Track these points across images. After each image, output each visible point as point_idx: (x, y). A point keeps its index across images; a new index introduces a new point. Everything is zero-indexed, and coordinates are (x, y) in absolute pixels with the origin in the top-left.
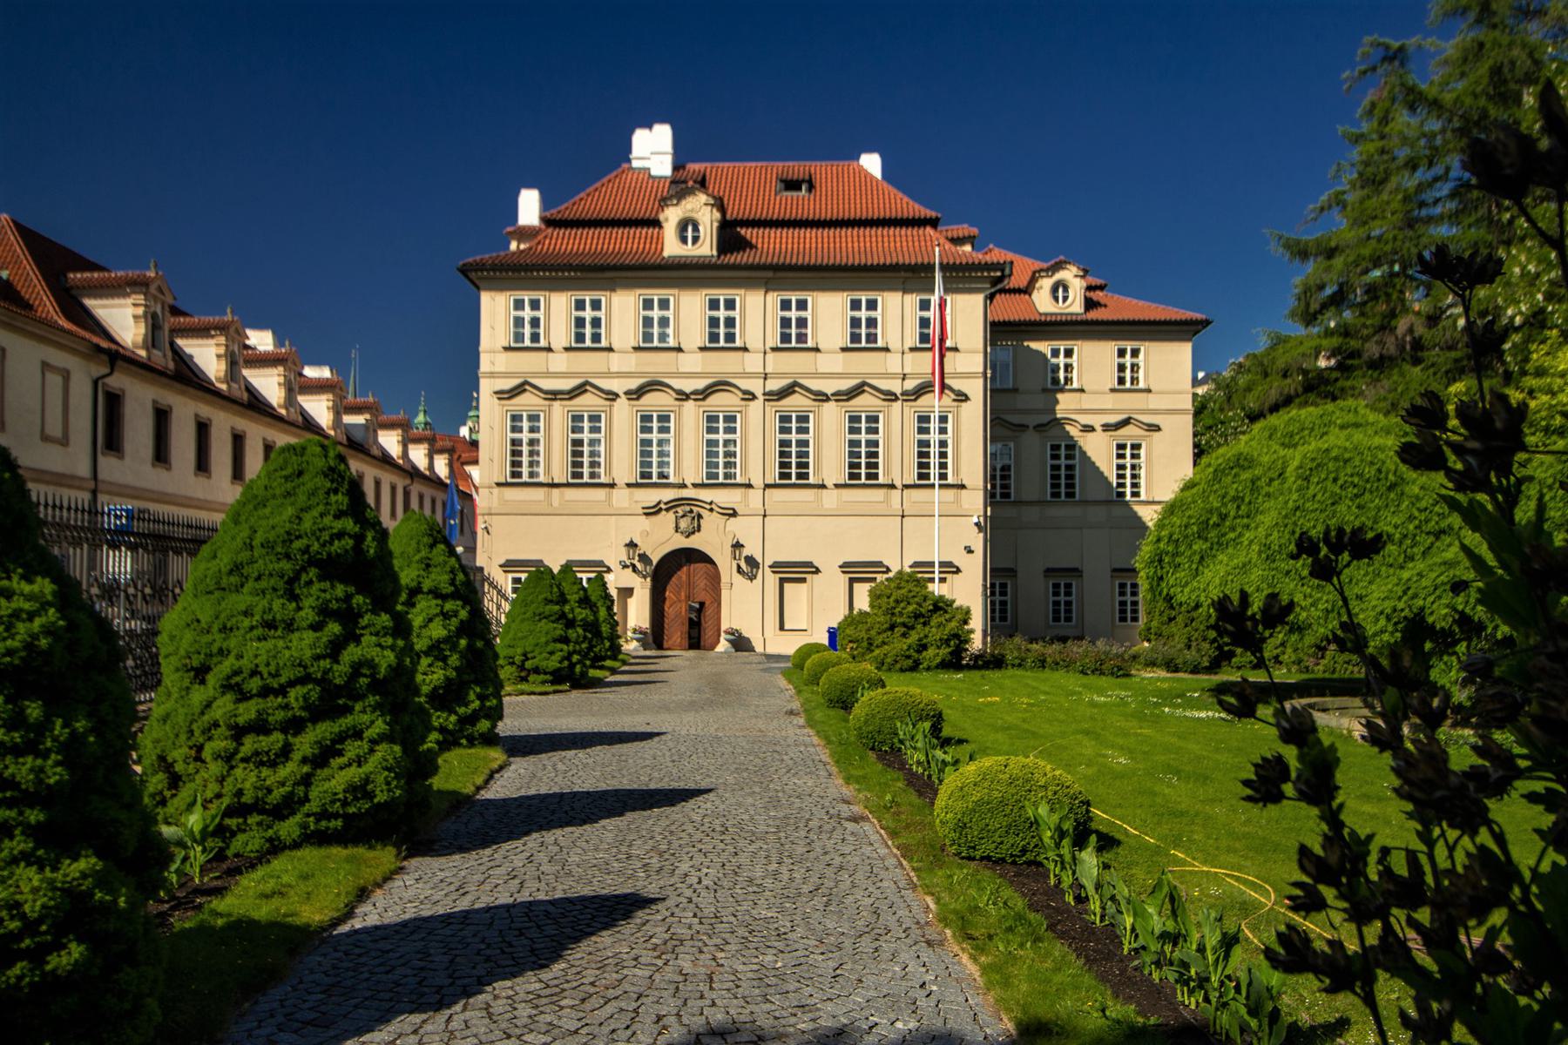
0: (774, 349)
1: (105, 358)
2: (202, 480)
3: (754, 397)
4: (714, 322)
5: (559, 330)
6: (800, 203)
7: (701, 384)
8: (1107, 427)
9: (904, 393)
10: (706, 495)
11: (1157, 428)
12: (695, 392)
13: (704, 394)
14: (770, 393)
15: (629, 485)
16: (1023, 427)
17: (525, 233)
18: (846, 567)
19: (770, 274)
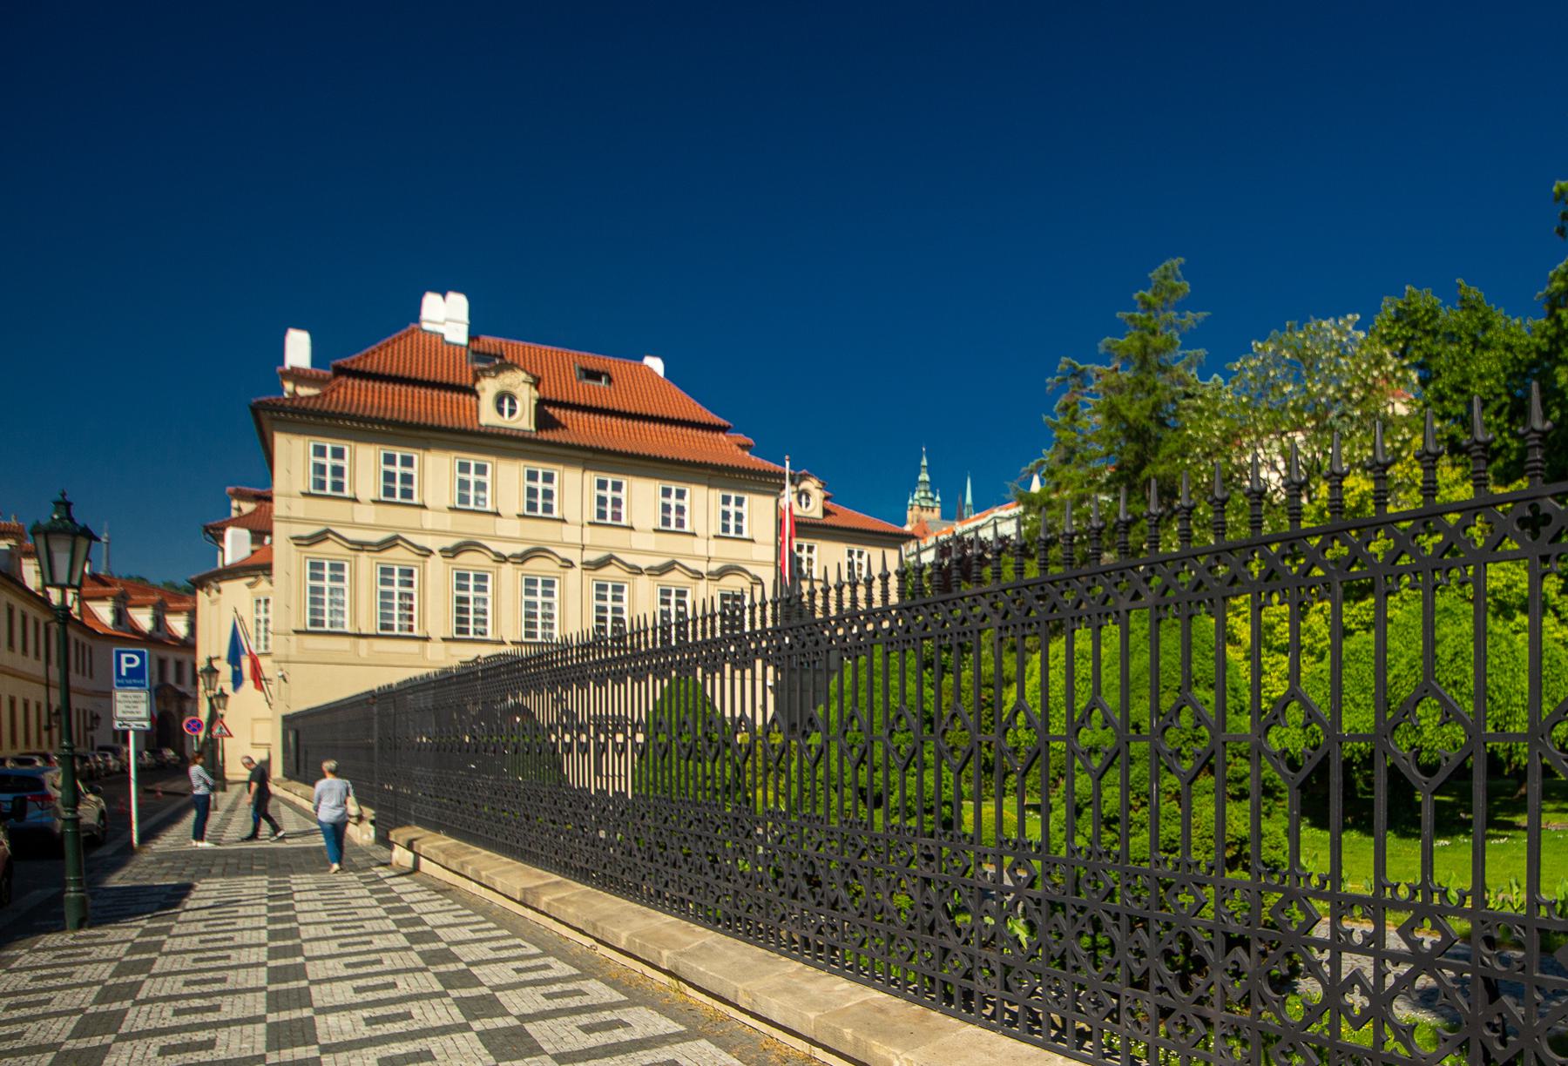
0: (592, 524)
3: (572, 565)
4: (532, 492)
7: (520, 549)
12: (514, 556)
13: (524, 557)
15: (444, 640)
19: (589, 455)
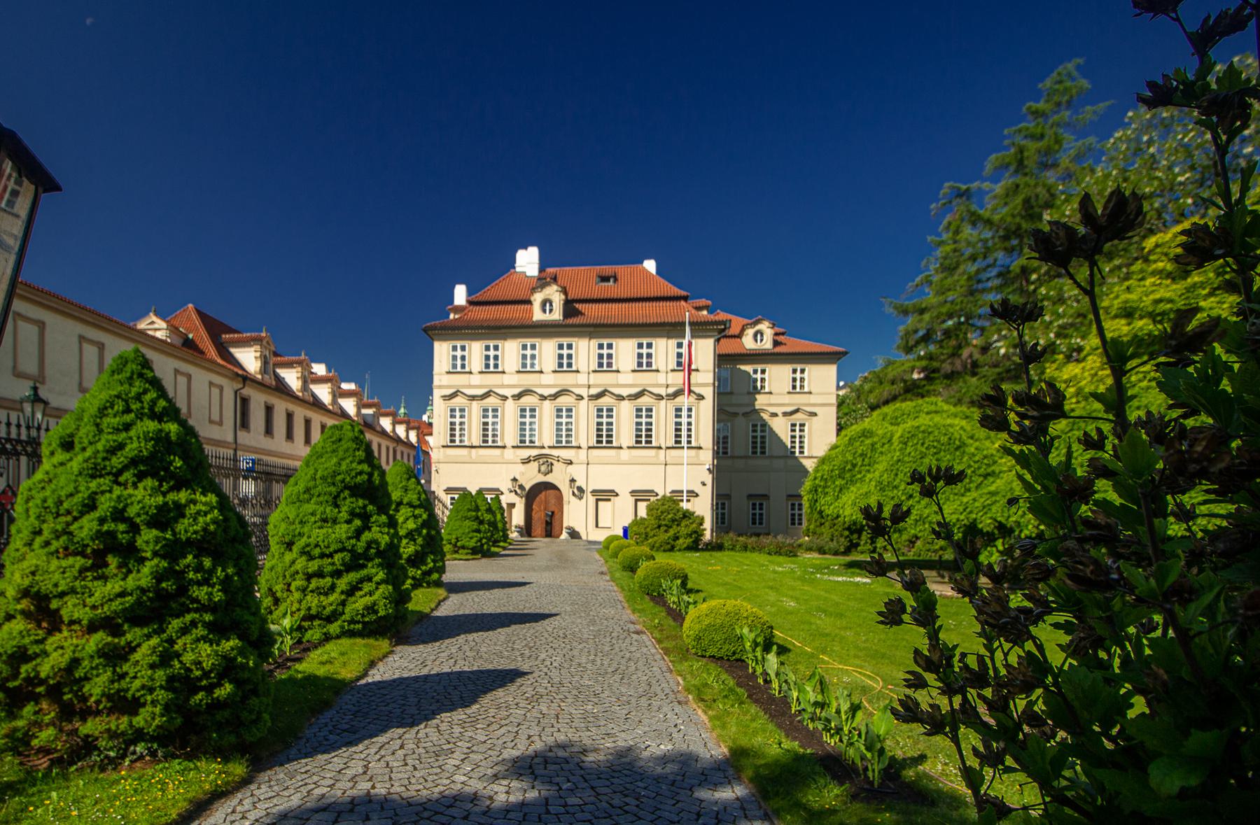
0: (595, 371)
1: (240, 379)
2: (289, 444)
3: (582, 398)
4: (561, 357)
5: (476, 363)
6: (610, 289)
7: (553, 391)
8: (785, 414)
9: (667, 395)
10: (555, 452)
11: (815, 414)
12: (550, 396)
13: (555, 396)
14: (592, 396)
15: (513, 447)
16: (735, 414)
17: (458, 309)
18: (633, 492)
19: (592, 329)
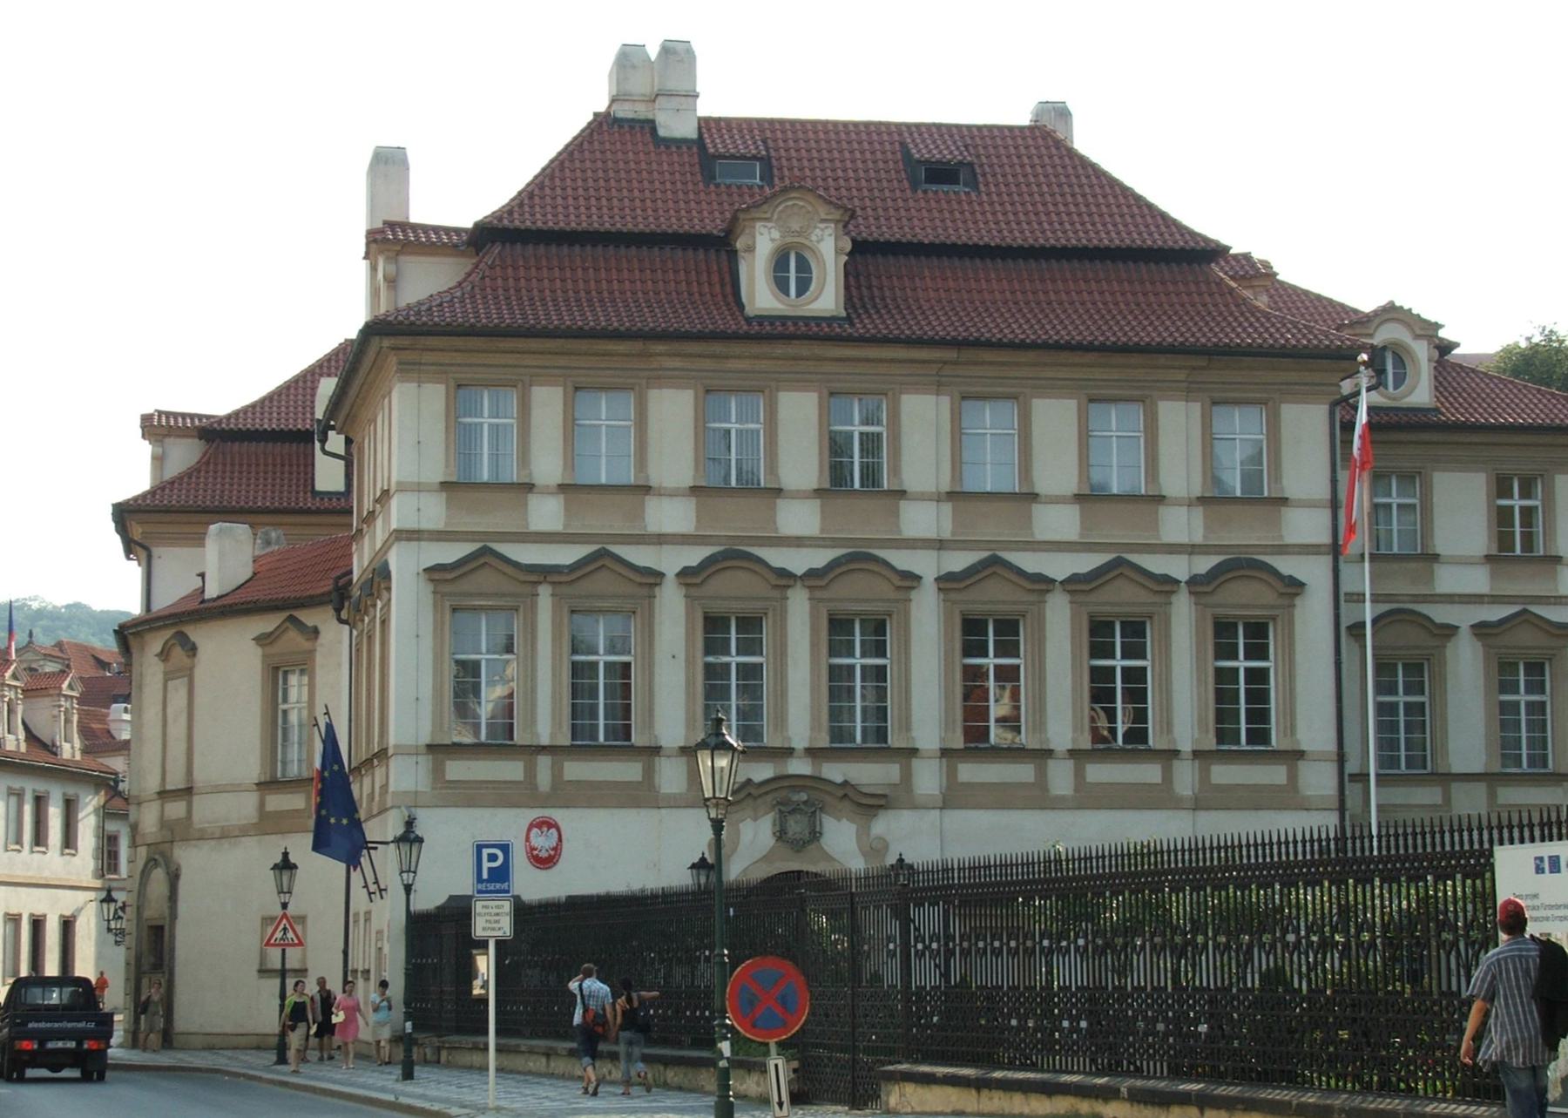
9: (1194, 581)
10: (835, 772)
12: (812, 574)
19: (951, 354)
